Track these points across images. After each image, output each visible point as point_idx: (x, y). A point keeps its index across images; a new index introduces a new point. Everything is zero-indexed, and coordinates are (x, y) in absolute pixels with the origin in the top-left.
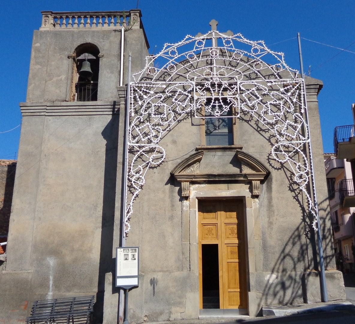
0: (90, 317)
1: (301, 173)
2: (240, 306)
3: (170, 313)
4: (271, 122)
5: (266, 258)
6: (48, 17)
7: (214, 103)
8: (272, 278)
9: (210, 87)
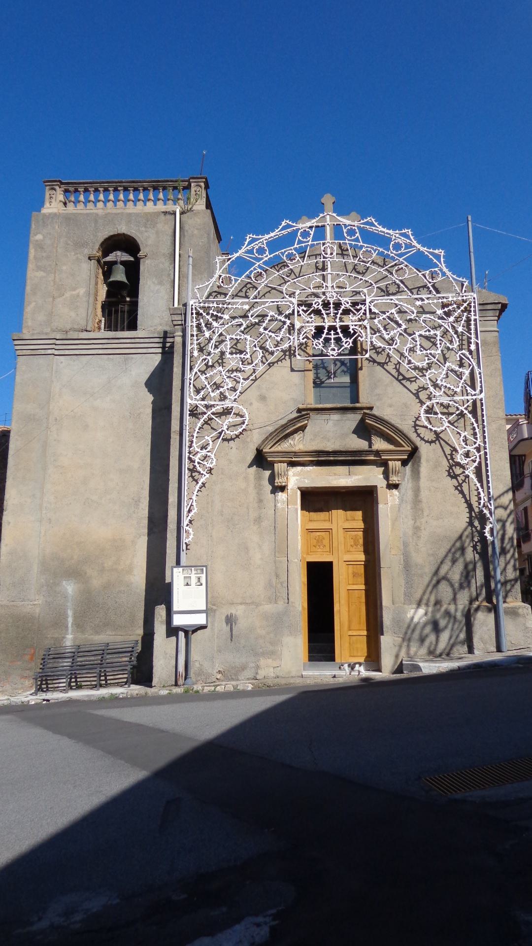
0: (132, 673)
1: (468, 448)
2: (367, 657)
3: (258, 667)
4: (421, 366)
5: (409, 584)
6: (55, 190)
7: (327, 334)
8: (419, 615)
9: (320, 307)
